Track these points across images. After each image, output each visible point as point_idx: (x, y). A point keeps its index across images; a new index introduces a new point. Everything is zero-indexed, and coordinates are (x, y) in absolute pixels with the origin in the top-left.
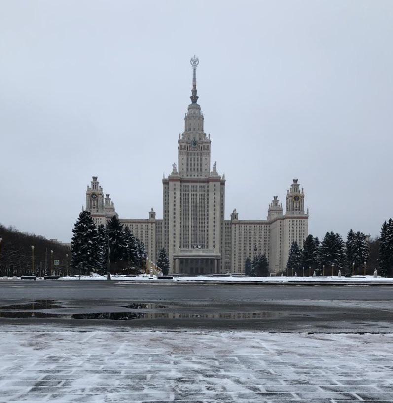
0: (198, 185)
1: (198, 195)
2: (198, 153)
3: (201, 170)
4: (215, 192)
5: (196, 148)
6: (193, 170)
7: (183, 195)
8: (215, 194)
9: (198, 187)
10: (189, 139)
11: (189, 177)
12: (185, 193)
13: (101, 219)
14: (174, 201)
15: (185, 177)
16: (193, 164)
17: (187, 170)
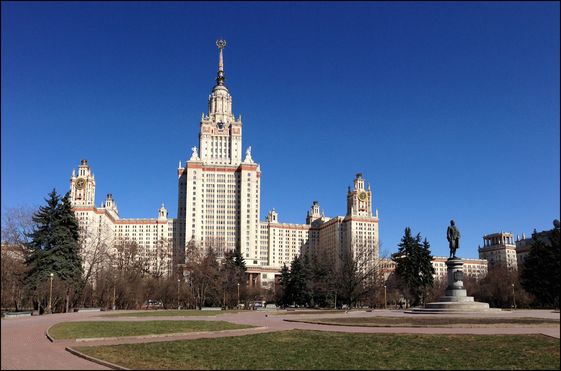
0: (227, 173)
1: (226, 186)
2: (225, 137)
3: (230, 156)
4: (249, 182)
5: (222, 131)
6: (219, 156)
7: (205, 185)
8: (249, 185)
9: (226, 176)
10: (214, 121)
11: (214, 163)
12: (208, 183)
13: (87, 213)
14: (194, 193)
15: (209, 163)
16: (219, 151)
17: (212, 156)
